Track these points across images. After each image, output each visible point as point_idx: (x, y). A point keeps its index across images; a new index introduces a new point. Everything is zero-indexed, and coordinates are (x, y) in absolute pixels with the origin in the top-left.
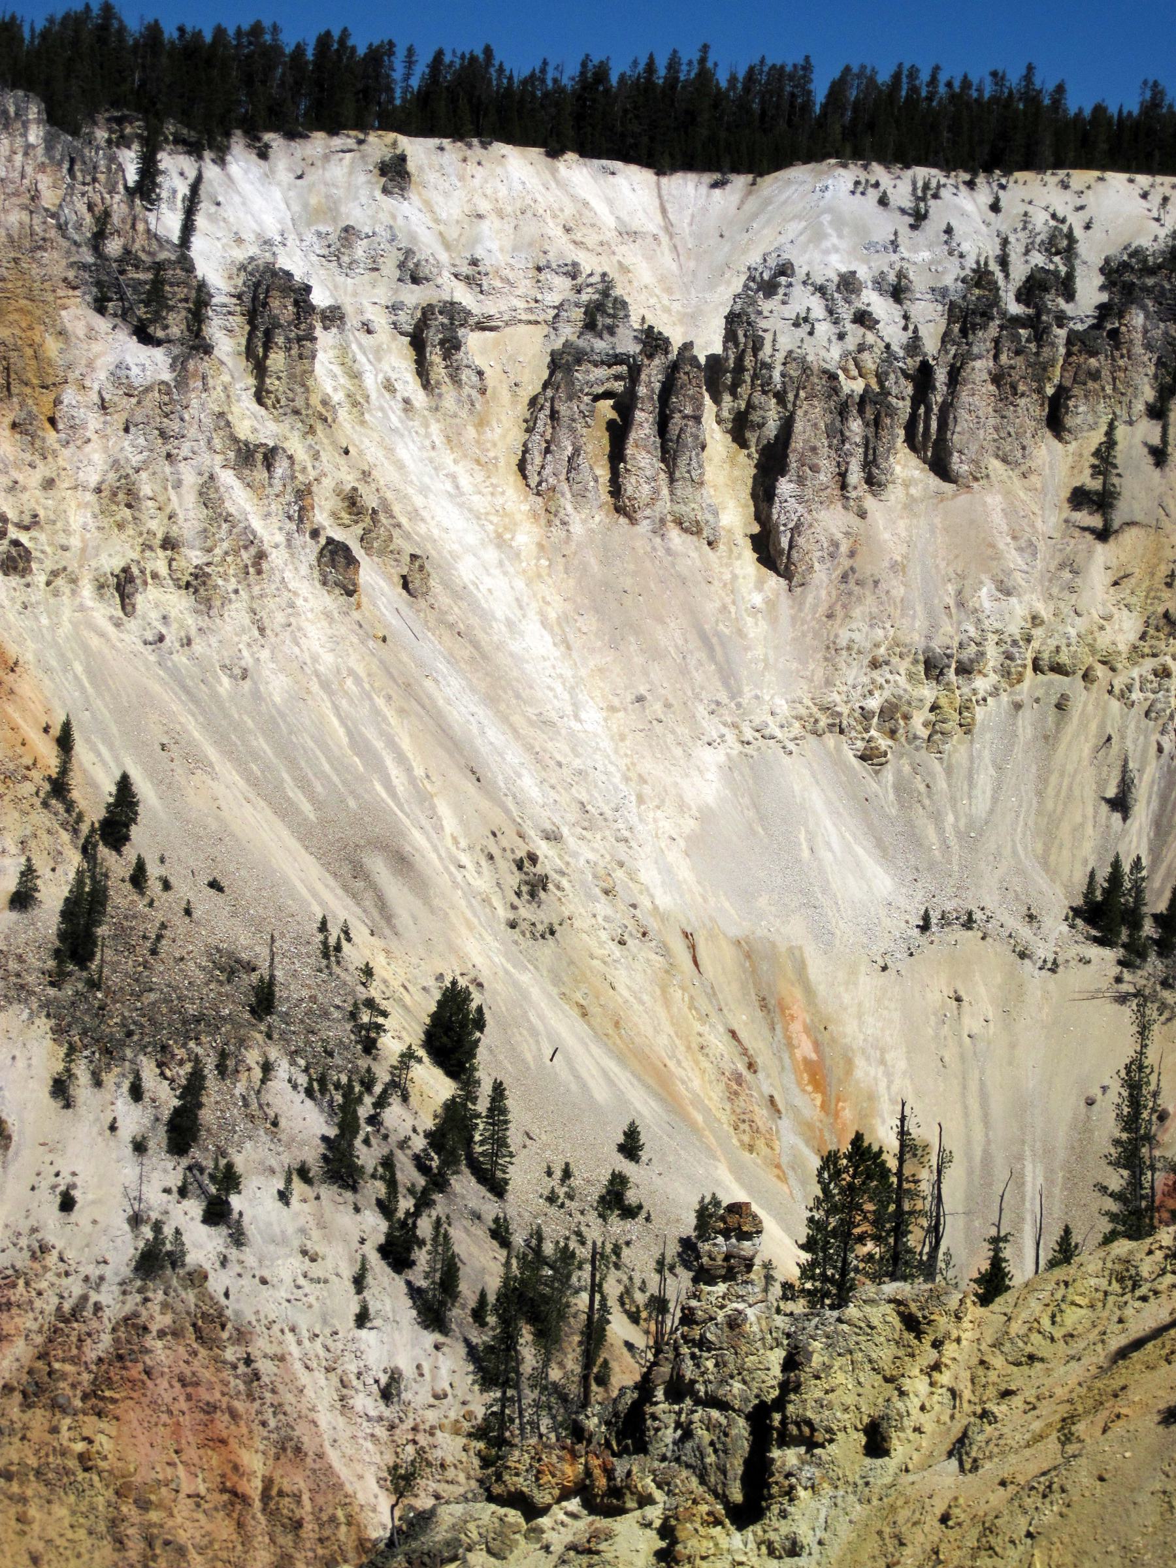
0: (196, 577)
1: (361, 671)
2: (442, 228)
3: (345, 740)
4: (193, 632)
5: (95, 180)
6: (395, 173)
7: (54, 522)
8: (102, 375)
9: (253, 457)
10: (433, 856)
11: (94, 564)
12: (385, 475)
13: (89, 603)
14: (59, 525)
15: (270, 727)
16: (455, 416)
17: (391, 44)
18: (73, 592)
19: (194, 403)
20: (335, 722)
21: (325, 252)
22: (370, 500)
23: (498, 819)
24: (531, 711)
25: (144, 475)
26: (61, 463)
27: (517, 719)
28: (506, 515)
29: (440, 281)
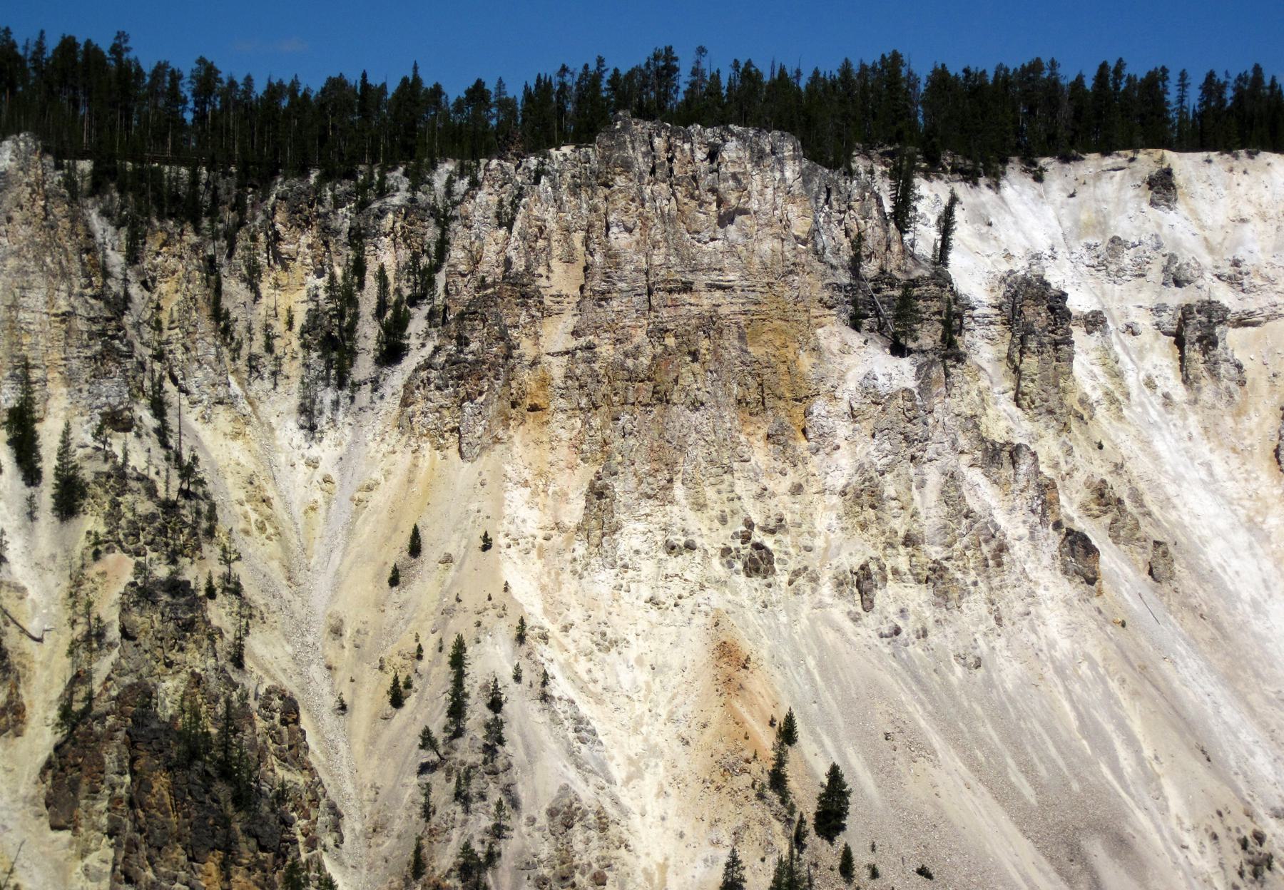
0: (934, 571)
1: (1097, 656)
2: (1207, 233)
3: (1074, 724)
4: (930, 624)
5: (850, 208)
6: (1162, 186)
7: (800, 525)
8: (852, 385)
9: (999, 456)
10: (1156, 837)
11: (835, 562)
12: (1139, 466)
13: (828, 600)
14: (804, 527)
15: (999, 714)
16: (1213, 407)
17: (1164, 70)
18: (814, 590)
19: (938, 408)
20: (1067, 706)
21: (1095, 262)
22: (1123, 492)
23: (1224, 797)
24: (1270, 690)
25: (888, 477)
26: (810, 468)
27: (1254, 698)
28: (1259, 499)
29: (1200, 282)
